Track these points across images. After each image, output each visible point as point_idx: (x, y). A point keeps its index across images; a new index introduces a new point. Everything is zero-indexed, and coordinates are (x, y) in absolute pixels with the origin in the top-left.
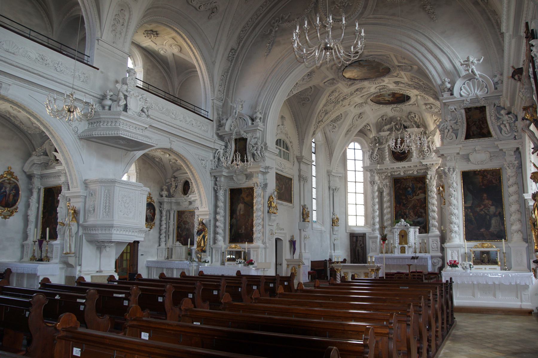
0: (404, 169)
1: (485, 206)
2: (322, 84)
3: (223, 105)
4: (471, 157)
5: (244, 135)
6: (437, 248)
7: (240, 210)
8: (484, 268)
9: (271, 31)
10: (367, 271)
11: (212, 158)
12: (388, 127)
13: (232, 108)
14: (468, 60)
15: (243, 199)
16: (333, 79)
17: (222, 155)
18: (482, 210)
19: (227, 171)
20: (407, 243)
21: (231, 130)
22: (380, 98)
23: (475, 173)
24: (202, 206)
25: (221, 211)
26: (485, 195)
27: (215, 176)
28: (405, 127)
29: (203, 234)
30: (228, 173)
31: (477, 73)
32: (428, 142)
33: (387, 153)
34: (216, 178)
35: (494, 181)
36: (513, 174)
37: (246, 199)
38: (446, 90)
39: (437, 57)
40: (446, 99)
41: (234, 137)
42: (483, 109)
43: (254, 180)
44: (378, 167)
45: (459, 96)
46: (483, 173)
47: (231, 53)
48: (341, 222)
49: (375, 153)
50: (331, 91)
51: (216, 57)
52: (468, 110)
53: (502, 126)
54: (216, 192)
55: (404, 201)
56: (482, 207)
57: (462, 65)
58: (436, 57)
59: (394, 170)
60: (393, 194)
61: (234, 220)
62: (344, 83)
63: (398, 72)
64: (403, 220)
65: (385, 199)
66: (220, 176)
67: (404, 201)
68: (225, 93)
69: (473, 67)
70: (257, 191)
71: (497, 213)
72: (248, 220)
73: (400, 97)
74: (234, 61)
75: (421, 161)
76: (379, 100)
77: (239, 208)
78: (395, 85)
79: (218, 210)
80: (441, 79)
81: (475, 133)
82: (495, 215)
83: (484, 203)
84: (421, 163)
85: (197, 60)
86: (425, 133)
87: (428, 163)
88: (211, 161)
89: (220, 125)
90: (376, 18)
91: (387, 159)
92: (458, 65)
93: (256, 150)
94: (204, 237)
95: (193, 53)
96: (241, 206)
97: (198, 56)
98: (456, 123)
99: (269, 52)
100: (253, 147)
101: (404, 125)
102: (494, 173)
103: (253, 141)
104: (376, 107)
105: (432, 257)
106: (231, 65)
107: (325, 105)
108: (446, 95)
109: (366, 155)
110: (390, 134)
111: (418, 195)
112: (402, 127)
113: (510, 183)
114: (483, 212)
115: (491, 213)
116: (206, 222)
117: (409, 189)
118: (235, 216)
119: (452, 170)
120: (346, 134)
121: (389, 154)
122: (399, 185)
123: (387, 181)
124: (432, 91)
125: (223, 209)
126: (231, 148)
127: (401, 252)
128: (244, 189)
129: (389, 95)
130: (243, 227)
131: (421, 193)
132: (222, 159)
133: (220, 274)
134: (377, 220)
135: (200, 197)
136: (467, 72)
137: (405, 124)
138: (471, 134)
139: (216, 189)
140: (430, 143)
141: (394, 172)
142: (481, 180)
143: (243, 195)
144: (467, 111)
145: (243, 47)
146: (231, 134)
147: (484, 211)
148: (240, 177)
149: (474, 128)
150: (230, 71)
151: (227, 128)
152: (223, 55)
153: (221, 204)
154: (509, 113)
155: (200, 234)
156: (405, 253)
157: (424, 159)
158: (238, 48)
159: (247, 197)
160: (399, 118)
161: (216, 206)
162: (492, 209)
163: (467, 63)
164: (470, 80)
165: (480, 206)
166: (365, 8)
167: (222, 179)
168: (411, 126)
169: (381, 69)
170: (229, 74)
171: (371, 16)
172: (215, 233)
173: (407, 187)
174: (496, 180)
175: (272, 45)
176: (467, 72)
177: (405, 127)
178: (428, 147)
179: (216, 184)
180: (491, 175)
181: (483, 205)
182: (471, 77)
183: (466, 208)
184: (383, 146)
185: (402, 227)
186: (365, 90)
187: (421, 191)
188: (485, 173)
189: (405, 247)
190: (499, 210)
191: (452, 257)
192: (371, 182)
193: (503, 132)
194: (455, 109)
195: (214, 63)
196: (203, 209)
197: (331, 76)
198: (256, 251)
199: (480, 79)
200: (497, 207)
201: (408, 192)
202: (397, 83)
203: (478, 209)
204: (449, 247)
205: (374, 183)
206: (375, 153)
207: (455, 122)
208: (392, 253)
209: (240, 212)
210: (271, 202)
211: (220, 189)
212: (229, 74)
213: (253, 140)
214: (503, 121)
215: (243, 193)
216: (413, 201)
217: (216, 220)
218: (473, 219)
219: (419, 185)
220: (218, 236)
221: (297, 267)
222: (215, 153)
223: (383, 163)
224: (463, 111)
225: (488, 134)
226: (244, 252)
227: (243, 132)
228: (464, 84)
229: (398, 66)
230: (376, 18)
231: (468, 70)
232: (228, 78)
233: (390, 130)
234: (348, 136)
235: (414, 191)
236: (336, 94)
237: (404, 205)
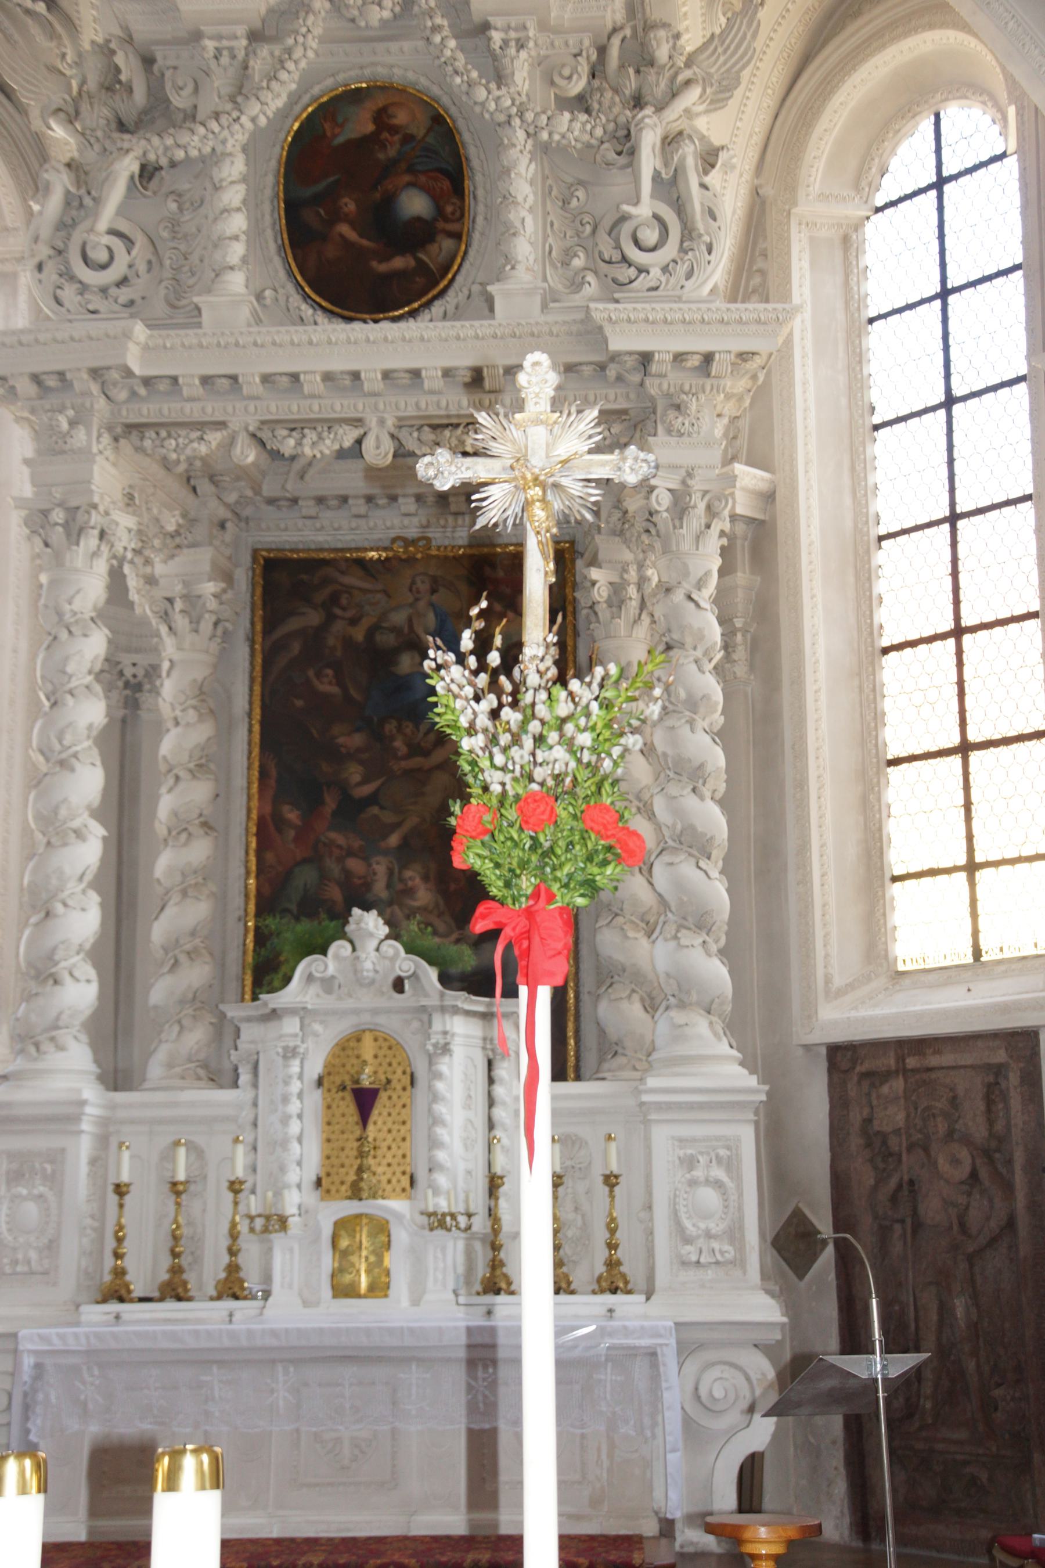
0: (409, 405)
6: (734, 1234)
33: (238, 223)
44: (138, 349)
49: (107, 216)
55: (354, 773)
59: (294, 408)
60: (241, 695)
64: (370, 924)
65: (167, 746)
67: (354, 773)
75: (600, 311)
84: (592, 333)
87: (663, 345)
91: (236, 282)
105: (692, 1340)
121: (254, 234)
122: (313, 618)
123: (203, 558)
127: (343, 1291)
134: (84, 920)
140: (689, 153)
141: (296, 427)
173: (386, 640)
178: (670, 187)
184: (194, 142)
185: (366, 999)
189: (381, 1228)
192: (38, 521)
205: (74, 531)
208: (232, 1287)
237: (351, 810)
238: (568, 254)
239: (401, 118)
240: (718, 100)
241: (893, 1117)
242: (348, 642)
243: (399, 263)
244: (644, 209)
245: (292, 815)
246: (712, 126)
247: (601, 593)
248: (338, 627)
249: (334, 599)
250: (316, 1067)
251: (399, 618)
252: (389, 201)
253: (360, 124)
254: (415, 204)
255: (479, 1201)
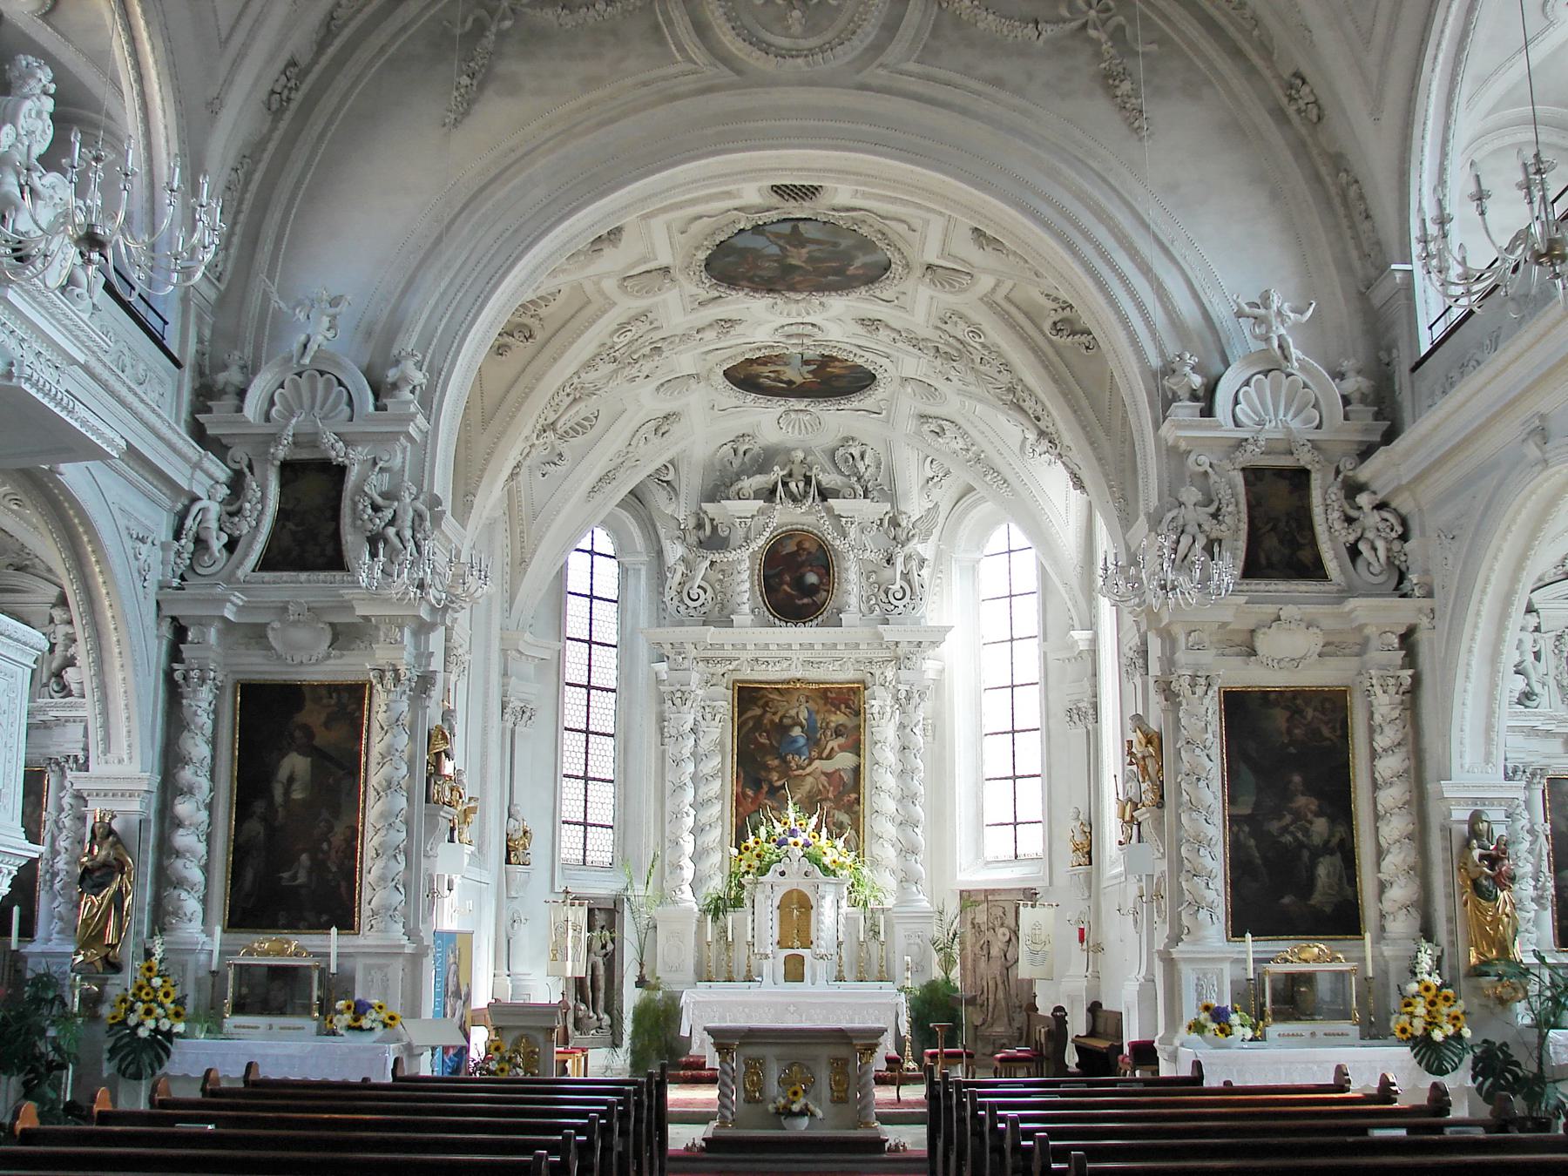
0: (807, 654)
1: (1298, 816)
2: (609, 285)
3: (222, 299)
4: (1262, 643)
5: (338, 452)
7: (291, 779)
8: (1307, 1034)
9: (480, 28)
10: (842, 1052)
11: (164, 533)
12: (759, 481)
13: (272, 326)
14: (1266, 299)
15: (309, 733)
16: (666, 270)
17: (214, 525)
18: (1285, 830)
19: (239, 598)
20: (807, 944)
21: (267, 419)
22: (765, 370)
23: (1266, 698)
24: (107, 750)
25: (194, 775)
26: (1297, 779)
27: (174, 619)
28: (824, 494)
29: (115, 886)
30: (240, 610)
31: (1295, 352)
32: (908, 558)
34: (179, 632)
35: (1326, 732)
36: (1396, 714)
37: (323, 738)
38: (1184, 393)
39: (1150, 270)
40: (1189, 427)
41: (282, 453)
42: (1299, 478)
43: (382, 655)
44: (712, 634)
45: (1231, 424)
46: (1292, 699)
47: (284, 78)
48: (538, 850)
49: (698, 581)
50: (632, 313)
51: (228, 82)
52: (1253, 475)
53: (1362, 546)
54: (174, 693)
56: (1288, 818)
57: (1240, 314)
58: (1146, 270)
61: (255, 827)
62: (691, 288)
63: (909, 285)
66: (202, 622)
67: (775, 776)
68: (232, 251)
69: (1282, 331)
70: (383, 706)
71: (1335, 840)
72: (331, 828)
73: (838, 376)
74: (288, 116)
76: (748, 378)
77: (283, 774)
78: (860, 330)
79: (186, 775)
80: (1162, 354)
81: (1275, 559)
82: (1326, 849)
83: (1293, 805)
85: (140, 78)
86: (895, 523)
88: (164, 547)
89: (204, 395)
90: (929, 78)
91: (746, 608)
92: (1221, 311)
93: (391, 523)
94: (118, 898)
95: (133, 41)
96: (296, 764)
97: (149, 60)
98: (1215, 516)
99: (466, 113)
100: (376, 508)
101: (818, 484)
102: (1327, 705)
103: (376, 484)
104: (731, 396)
106: (272, 130)
107: (589, 365)
108: (1185, 410)
109: (631, 581)
110: (761, 512)
111: (829, 757)
112: (813, 490)
113: (1381, 742)
114: (1289, 838)
115: (1317, 840)
116: (127, 822)
117: (797, 731)
118: (259, 806)
119: (1202, 681)
120: (593, 490)
122: (758, 711)
124: (1005, 378)
125: (205, 770)
126: (263, 499)
128: (313, 687)
129: (806, 363)
130: (304, 857)
131: (842, 748)
132: (217, 543)
133: (356, 1078)
135: (105, 713)
136: (1263, 346)
137: (829, 479)
138: (1263, 561)
139: (178, 676)
140: (914, 564)
142: (1283, 725)
143: (312, 716)
144: (1251, 478)
145: (339, 62)
146: (274, 438)
147: (1292, 833)
148: (301, 635)
149: (1271, 542)
150: (267, 156)
151: (252, 407)
152: (258, 78)
153: (198, 748)
154: (1381, 506)
155: (98, 888)
156: (800, 978)
157: (886, 622)
158: (314, 62)
159: (326, 725)
160: (800, 455)
161: (171, 758)
162: (1320, 826)
163: (1257, 313)
164: (1266, 373)
165: (1281, 817)
166: (890, 28)
167: (212, 635)
168: (848, 491)
169: (858, 263)
170: (262, 167)
171: (912, 66)
172: (165, 880)
173: (787, 721)
174: (1334, 729)
175: (481, 87)
176: (1263, 346)
177: (824, 494)
179: (175, 655)
180: (1315, 710)
181: (1291, 811)
182: (1273, 365)
183: (1234, 821)
184: (732, 556)
186: (739, 329)
187: (841, 740)
188: (1299, 702)
190: (1340, 831)
191: (1199, 994)
193: (1360, 563)
194: (1211, 465)
195: (214, 106)
196: (114, 769)
197: (664, 259)
198: (380, 967)
199: (1300, 377)
200: (1333, 820)
201: (794, 740)
202: (871, 324)
203: (1274, 826)
204: (1185, 960)
206: (698, 581)
207: (1212, 509)
209: (287, 792)
210: (438, 755)
211: (203, 680)
212: (262, 167)
213: (373, 478)
214: (1364, 530)
215: (309, 705)
216: (810, 779)
217: (167, 820)
218: (1259, 861)
219: (838, 718)
220: (184, 895)
221: (541, 1037)
222: (182, 517)
223: (730, 624)
224: (1239, 479)
225: (1315, 571)
226: (323, 972)
227: (332, 438)
228: (1247, 383)
229: (929, 267)
230: (929, 78)
231: (1268, 340)
232: (253, 187)
233: (770, 494)
234: (598, 497)
235: (813, 741)
236: (637, 329)
238: (869, 599)
239: (807, 545)
240: (925, 540)
241: (981, 918)
242: (772, 721)
243: (805, 601)
244: (897, 587)
245: (750, 793)
246: (921, 548)
247: (875, 710)
248: (768, 715)
249: (766, 704)
250: (777, 903)
251: (793, 713)
252: (802, 576)
253: (791, 547)
254: (812, 578)
255: (833, 951)
